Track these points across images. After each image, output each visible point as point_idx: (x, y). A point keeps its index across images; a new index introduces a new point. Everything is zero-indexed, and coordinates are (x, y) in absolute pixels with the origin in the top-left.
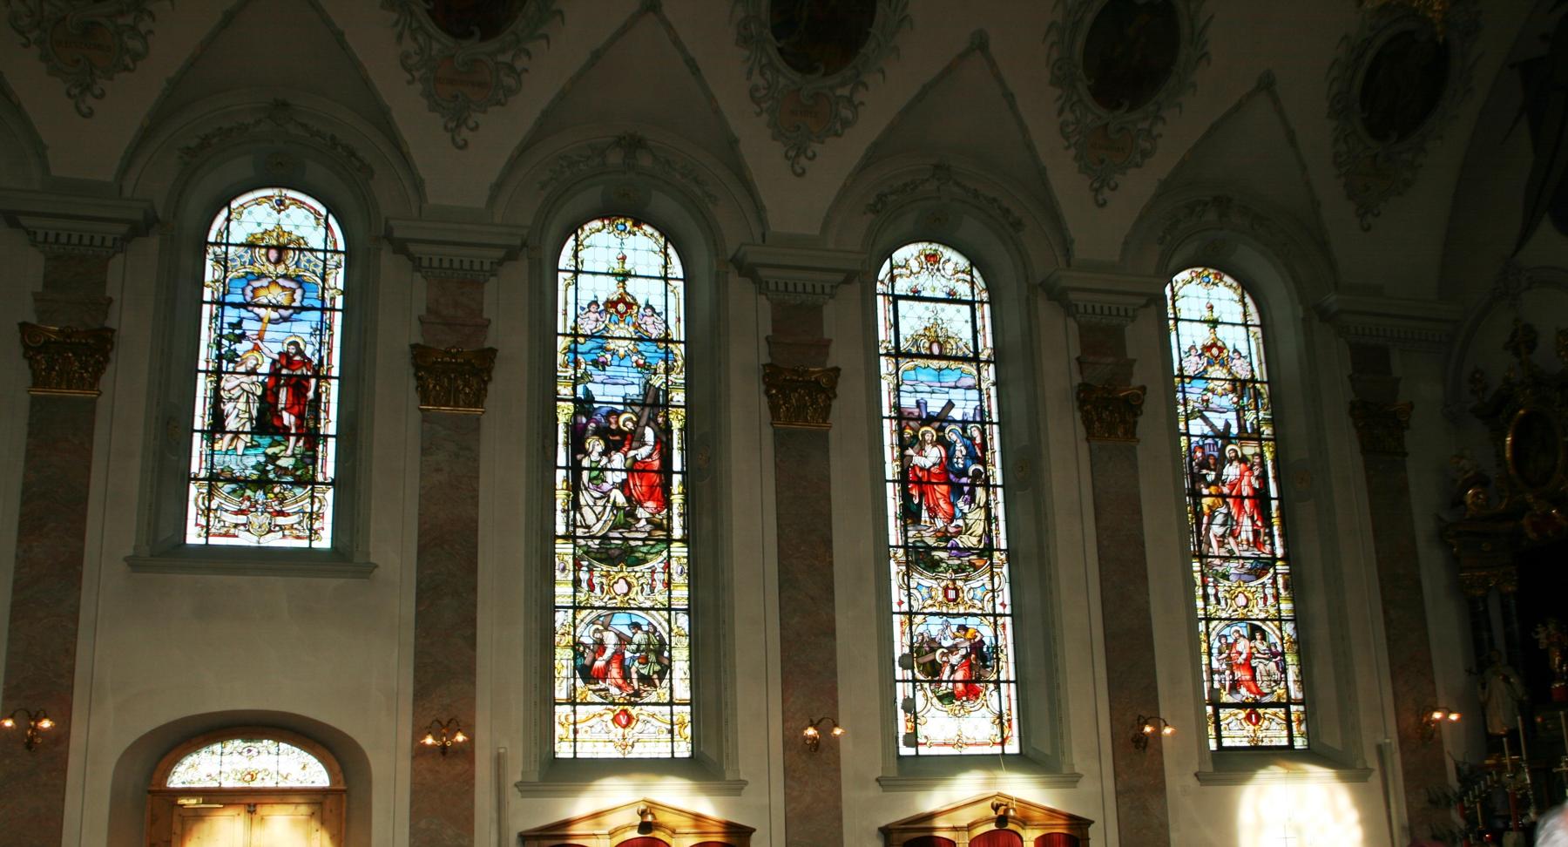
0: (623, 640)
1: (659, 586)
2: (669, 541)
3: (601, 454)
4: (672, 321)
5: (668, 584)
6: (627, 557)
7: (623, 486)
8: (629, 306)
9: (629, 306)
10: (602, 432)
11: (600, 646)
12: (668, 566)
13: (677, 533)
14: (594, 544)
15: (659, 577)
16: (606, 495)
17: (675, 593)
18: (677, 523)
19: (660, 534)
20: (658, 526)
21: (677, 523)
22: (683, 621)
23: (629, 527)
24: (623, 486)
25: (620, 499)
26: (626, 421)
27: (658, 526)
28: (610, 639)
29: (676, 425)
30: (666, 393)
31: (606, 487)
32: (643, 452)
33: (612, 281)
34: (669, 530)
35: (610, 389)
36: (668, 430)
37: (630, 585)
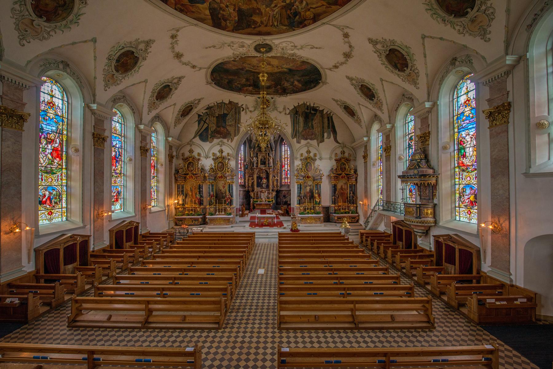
0: (50, 193)
1: (60, 180)
2: (62, 169)
3: (45, 144)
4: (64, 112)
5: (61, 179)
6: (51, 172)
7: (51, 154)
8: (53, 105)
9: (53, 105)
10: (46, 138)
11: (45, 196)
12: (62, 175)
13: (64, 167)
14: (43, 168)
15: (59, 177)
16: (46, 155)
17: (63, 181)
18: (64, 164)
19: (60, 167)
20: (60, 165)
21: (64, 164)
22: (65, 188)
23: (52, 164)
24: (51, 154)
25: (50, 157)
26: (52, 136)
27: (60, 165)
28: (47, 193)
29: (64, 139)
30: (62, 131)
31: (46, 153)
32: (56, 145)
33: (49, 97)
34: (62, 166)
35: (48, 127)
36: (62, 141)
37: (52, 180)
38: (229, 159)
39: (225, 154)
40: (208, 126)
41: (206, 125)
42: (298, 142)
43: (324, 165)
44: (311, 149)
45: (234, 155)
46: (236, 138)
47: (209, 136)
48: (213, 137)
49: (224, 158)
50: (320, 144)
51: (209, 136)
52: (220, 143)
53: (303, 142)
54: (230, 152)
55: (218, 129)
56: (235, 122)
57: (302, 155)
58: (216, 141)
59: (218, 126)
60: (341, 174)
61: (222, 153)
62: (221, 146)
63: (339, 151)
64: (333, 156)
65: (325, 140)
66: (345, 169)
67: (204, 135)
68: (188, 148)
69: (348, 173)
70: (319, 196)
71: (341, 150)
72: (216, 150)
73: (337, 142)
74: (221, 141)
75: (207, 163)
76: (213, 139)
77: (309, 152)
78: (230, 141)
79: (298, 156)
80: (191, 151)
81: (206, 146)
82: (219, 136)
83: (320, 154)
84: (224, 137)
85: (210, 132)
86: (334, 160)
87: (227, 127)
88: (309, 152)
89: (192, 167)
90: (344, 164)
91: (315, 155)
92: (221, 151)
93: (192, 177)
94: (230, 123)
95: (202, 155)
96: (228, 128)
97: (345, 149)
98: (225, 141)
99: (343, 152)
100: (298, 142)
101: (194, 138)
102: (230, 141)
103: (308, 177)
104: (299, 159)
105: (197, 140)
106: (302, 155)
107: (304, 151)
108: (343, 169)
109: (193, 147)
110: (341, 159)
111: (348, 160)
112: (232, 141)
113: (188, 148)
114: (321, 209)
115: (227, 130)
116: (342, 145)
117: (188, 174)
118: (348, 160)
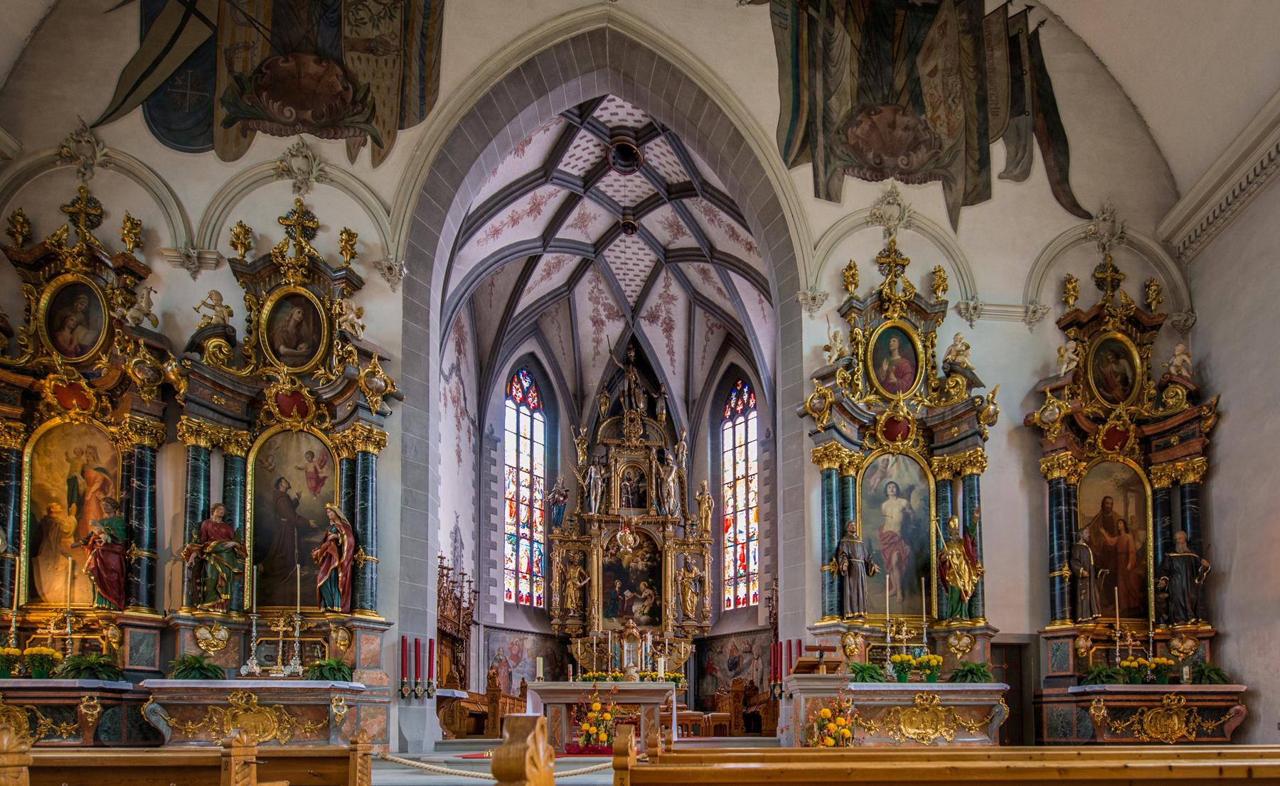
38: (354, 284)
39: (325, 245)
40: (211, 43)
41: (195, 35)
42: (827, 192)
43: (1005, 353)
44: (906, 241)
45: (397, 253)
46: (406, 139)
47: (221, 113)
48: (247, 120)
49: (314, 269)
50: (967, 213)
51: (221, 113)
52: (297, 163)
53: (859, 193)
54: (369, 235)
55: (286, 65)
56: (407, 25)
57: (848, 276)
58: (266, 148)
59: (284, 47)
60: (1104, 422)
61: (310, 233)
62: (297, 188)
63: (1082, 267)
64: (1048, 297)
65: (999, 187)
66: (1127, 384)
67: (190, 107)
68: (64, 187)
69: (1146, 410)
70: (973, 555)
71: (1098, 258)
72: (265, 214)
73: (1073, 207)
74: (302, 151)
75: (186, 296)
76: (246, 135)
77: (891, 261)
78: (366, 153)
79: (827, 283)
80: (87, 212)
81: (199, 178)
82: (289, 113)
83: (965, 277)
84: (329, 126)
85: (224, 80)
86: (1050, 323)
87: (350, 58)
88: (891, 261)
89: (86, 323)
90: (1121, 353)
91: (935, 281)
92: (303, 224)
93: (74, 388)
94: (369, 32)
95: (166, 241)
96: (358, 64)
97: (1122, 259)
98: (333, 150)
99: (1108, 279)
100: (827, 192)
101: (110, 116)
102: (366, 153)
103: (893, 429)
104: (834, 302)
105: (132, 135)
106: (848, 276)
107: (863, 249)
108: (1118, 387)
109: (105, 186)
110: (1098, 317)
111: (1142, 324)
112: (378, 159)
113: (64, 187)
114: (981, 655)
115: (348, 76)
116: (1104, 228)
117: (48, 370)
118: (1142, 324)
